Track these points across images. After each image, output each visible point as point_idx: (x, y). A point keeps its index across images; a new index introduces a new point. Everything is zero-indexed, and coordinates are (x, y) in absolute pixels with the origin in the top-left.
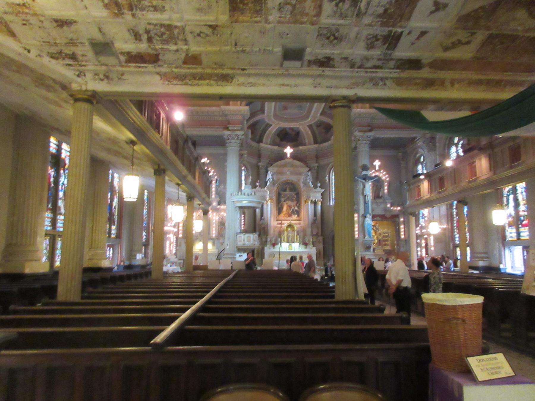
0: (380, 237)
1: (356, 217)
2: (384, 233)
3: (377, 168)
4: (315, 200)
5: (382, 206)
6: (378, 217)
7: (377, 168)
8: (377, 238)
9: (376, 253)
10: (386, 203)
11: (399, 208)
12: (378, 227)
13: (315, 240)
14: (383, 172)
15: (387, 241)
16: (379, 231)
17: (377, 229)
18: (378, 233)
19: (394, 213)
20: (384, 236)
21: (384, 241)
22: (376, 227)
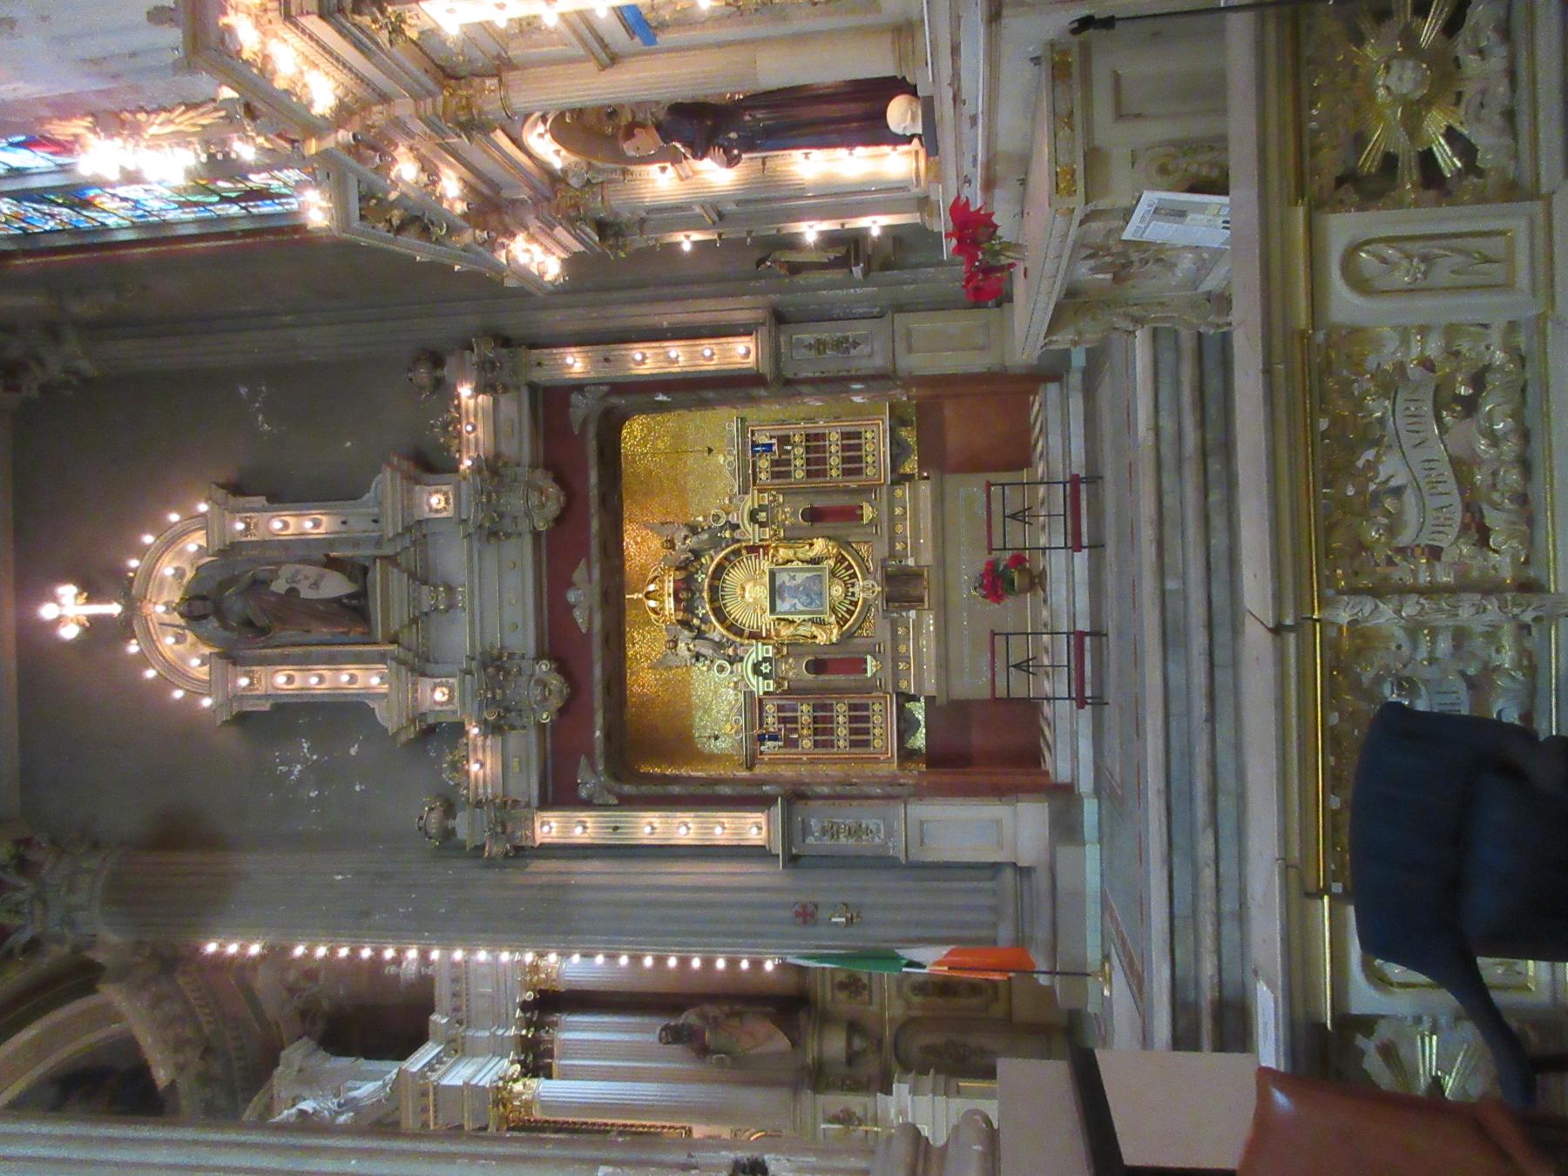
0: (790, 513)
1: (566, 828)
2: (749, 481)
3: (114, 609)
4: (525, 1006)
5: (453, 558)
6: (572, 597)
7: (114, 609)
8: (791, 539)
9: (927, 558)
10: (419, 531)
11: (465, 391)
12: (694, 530)
13: (835, 1045)
14: (141, 552)
15: (814, 441)
16: (735, 527)
17: (716, 543)
18: (751, 533)
19: (520, 447)
20: (781, 469)
21: (816, 465)
22: (697, 554)
